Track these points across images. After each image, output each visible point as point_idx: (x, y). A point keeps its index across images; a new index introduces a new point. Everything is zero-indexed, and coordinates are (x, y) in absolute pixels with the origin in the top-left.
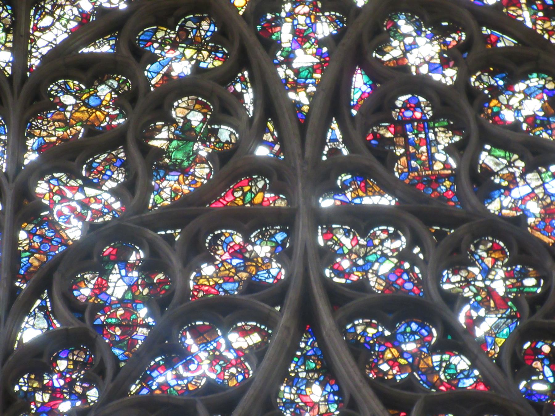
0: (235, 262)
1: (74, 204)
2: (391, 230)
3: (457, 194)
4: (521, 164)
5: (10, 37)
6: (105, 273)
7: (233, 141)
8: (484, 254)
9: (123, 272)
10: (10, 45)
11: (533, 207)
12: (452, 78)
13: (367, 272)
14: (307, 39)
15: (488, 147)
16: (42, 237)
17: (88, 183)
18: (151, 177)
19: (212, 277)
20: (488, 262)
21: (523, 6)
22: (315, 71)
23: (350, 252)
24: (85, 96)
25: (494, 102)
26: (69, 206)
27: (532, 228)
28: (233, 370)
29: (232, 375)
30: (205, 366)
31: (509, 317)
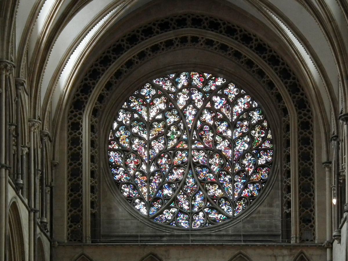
0: (180, 157)
4: (222, 139)
6: (162, 159)
14: (191, 114)
16: (153, 152)
20: (216, 158)
28: (180, 176)
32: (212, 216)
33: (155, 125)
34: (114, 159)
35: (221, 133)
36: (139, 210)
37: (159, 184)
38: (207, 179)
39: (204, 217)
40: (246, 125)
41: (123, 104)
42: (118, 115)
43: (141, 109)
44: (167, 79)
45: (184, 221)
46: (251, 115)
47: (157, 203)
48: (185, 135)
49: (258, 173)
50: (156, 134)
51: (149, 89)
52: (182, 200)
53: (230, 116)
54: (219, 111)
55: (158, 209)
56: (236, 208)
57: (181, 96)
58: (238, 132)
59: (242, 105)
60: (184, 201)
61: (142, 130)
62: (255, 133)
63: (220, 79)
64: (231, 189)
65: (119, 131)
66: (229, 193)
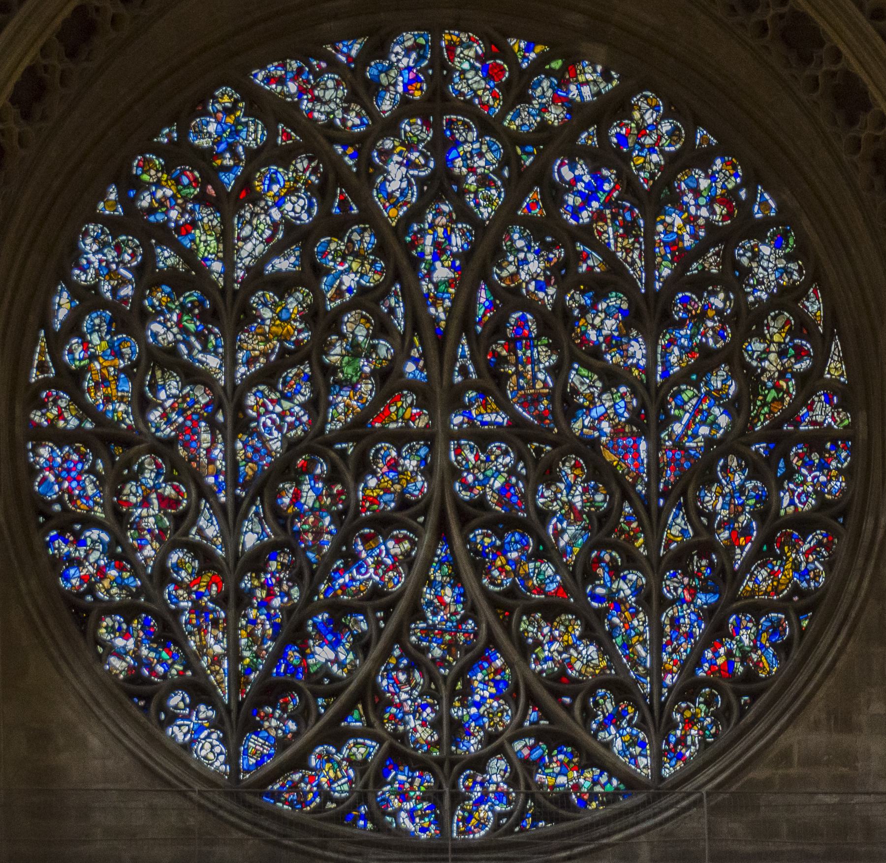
0: (392, 474)
1: (274, 416)
2: (504, 446)
3: (553, 413)
4: (599, 384)
5: (221, 246)
6: (299, 483)
7: (389, 357)
8: (569, 471)
9: (312, 482)
10: (221, 255)
11: (605, 426)
12: (552, 296)
13: (485, 487)
14: (444, 251)
15: (576, 366)
16: (252, 447)
17: (285, 397)
18: (329, 393)
19: (375, 488)
20: (571, 478)
21: (609, 221)
22: (450, 286)
23: (474, 467)
24: (279, 309)
25: (582, 321)
26: (270, 418)
27: (604, 446)
29: (390, 578)
30: (372, 571)
31: (584, 529)
32: (549, 781)
33: (265, 305)
34: (60, 484)
35: (596, 352)
36: (187, 747)
37: (288, 611)
38: (528, 589)
39: (512, 781)
40: (719, 312)
41: (103, 196)
42: (75, 254)
43: (193, 224)
44: (323, 65)
45: (408, 806)
46: (745, 261)
47: (278, 713)
48: (416, 361)
49: (777, 557)
50: (264, 354)
51: (230, 120)
52: (404, 696)
53: (639, 263)
54: (586, 234)
55: (281, 744)
56: (673, 739)
57: (396, 158)
58: (681, 347)
59: (698, 207)
60: (414, 701)
61: (198, 335)
62: (766, 351)
63: (589, 69)
64: (643, 643)
65: (86, 344)
66: (636, 662)
